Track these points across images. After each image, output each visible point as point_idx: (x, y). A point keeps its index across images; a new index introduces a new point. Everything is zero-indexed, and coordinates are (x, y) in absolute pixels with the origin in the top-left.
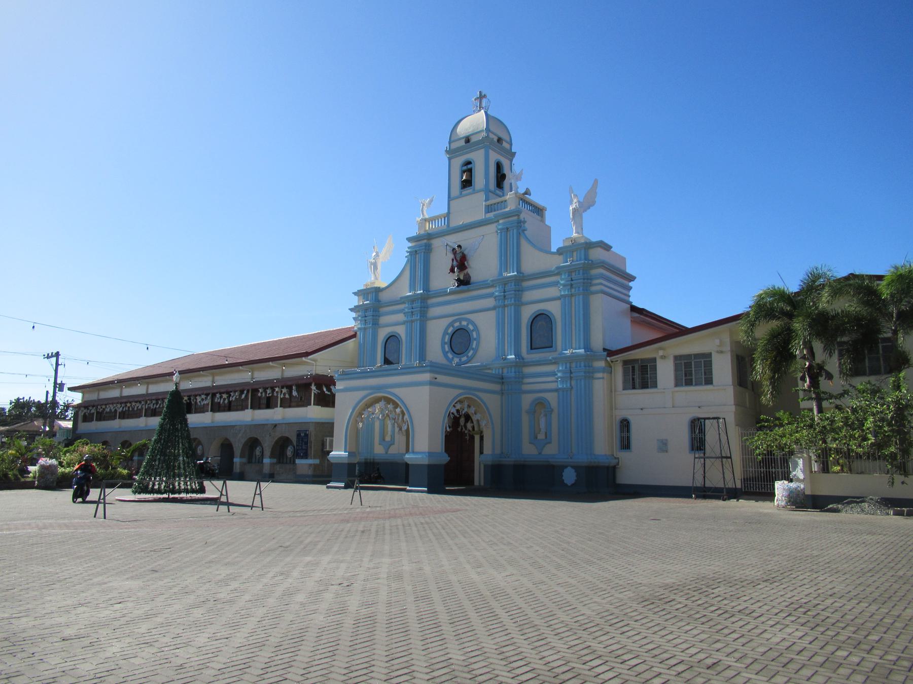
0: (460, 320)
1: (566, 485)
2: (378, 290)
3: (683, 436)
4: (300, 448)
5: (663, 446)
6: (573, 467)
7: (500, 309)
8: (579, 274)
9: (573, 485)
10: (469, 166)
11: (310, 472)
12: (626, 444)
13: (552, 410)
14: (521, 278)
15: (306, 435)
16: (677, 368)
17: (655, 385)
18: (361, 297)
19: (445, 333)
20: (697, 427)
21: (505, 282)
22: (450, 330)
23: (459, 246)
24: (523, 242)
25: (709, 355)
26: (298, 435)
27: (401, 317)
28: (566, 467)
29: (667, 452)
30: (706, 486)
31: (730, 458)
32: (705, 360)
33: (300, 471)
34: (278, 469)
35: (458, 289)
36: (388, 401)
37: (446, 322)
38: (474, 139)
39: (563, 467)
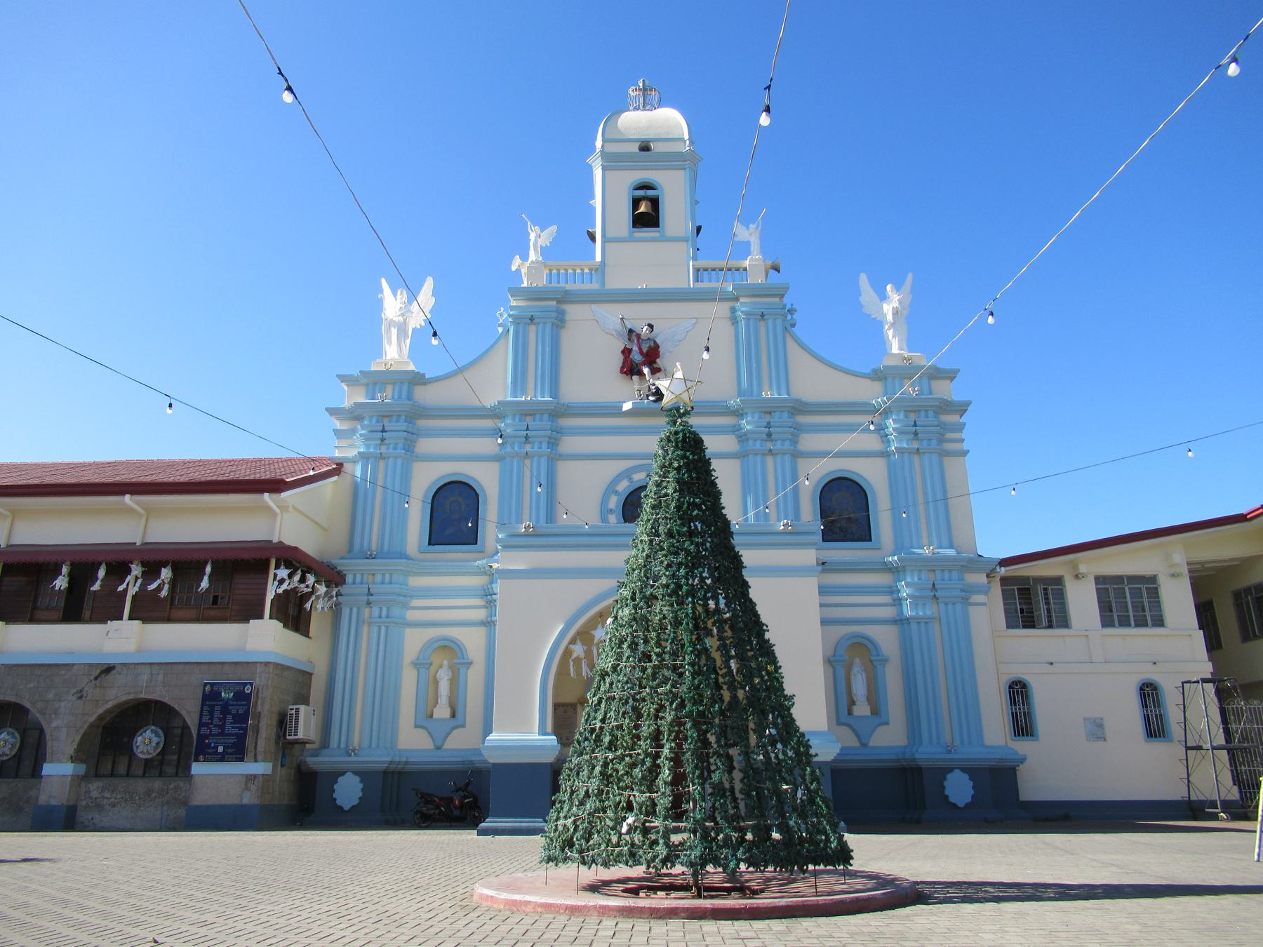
1: (954, 805)
3: (1131, 713)
4: (215, 731)
5: (1097, 730)
6: (964, 770)
7: (759, 458)
8: (927, 416)
9: (967, 805)
10: (650, 193)
11: (249, 798)
12: (1023, 726)
13: (885, 661)
14: (799, 408)
15: (242, 697)
17: (1065, 623)
18: (362, 390)
19: (610, 489)
20: (1149, 693)
21: (768, 409)
23: (651, 326)
24: (791, 344)
25: (1153, 579)
26: (210, 697)
28: (951, 770)
29: (1105, 740)
30: (1192, 798)
31: (1188, 748)
32: (1147, 587)
33: (202, 797)
34: (95, 794)
37: (614, 468)
38: (656, 147)
39: (941, 772)
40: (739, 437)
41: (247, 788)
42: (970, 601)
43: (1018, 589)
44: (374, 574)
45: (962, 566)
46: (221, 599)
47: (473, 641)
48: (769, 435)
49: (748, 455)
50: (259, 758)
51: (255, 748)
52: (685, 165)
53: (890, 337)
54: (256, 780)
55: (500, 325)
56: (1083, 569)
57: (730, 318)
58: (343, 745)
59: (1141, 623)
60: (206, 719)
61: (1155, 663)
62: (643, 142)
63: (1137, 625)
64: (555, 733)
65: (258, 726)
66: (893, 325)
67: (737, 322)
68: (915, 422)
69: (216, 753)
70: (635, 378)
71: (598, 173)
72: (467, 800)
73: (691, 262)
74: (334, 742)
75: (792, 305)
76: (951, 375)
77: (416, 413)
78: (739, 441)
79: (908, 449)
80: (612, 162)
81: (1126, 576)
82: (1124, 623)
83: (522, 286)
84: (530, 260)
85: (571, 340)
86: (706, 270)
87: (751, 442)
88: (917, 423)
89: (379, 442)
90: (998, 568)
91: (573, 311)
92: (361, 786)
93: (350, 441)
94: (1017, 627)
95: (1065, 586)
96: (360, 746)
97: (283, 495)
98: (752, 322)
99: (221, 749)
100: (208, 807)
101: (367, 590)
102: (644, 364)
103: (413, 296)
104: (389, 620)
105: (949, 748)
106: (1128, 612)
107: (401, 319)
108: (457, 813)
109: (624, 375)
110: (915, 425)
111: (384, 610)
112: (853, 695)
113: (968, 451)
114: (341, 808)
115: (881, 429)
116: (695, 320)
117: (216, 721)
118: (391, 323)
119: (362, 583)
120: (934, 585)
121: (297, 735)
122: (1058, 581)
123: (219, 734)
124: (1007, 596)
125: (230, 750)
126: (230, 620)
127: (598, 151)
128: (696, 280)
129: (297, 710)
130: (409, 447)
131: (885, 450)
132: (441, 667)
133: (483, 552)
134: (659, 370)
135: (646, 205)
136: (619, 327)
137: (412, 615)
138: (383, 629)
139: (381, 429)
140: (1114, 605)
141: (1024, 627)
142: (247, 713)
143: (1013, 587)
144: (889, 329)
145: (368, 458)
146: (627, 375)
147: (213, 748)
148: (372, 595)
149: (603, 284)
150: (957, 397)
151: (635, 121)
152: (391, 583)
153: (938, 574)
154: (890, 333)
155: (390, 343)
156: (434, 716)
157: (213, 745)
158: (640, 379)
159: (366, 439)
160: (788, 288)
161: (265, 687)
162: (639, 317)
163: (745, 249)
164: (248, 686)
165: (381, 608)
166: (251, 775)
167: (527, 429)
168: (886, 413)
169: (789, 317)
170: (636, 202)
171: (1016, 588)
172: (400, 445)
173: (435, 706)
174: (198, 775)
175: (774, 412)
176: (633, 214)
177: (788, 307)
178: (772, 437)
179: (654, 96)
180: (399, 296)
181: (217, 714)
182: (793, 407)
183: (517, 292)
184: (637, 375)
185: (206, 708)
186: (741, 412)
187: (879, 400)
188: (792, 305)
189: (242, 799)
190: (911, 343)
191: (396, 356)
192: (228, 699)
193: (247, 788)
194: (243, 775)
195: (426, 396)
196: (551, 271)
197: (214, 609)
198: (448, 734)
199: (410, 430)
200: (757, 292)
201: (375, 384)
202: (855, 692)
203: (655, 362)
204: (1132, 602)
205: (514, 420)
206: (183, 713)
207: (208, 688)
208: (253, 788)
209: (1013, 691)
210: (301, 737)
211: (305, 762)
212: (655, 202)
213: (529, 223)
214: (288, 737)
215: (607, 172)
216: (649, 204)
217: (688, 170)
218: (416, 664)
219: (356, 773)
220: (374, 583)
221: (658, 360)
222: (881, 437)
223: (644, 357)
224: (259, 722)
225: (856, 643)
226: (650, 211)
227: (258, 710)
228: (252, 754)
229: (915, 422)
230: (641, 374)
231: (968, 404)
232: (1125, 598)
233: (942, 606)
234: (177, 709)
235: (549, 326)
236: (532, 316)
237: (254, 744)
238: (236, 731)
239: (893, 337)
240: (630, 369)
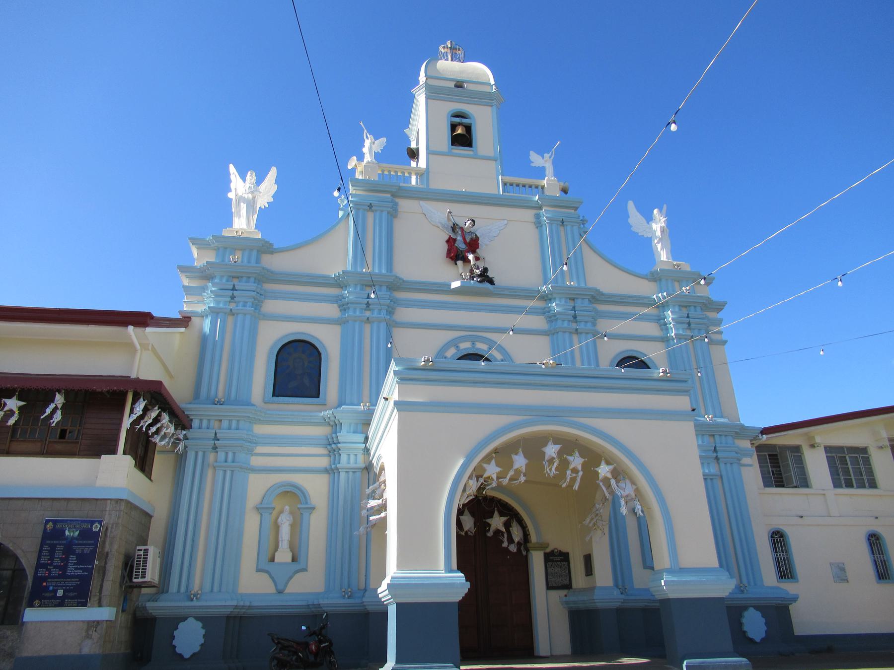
1: (751, 641)
4: (55, 572)
5: (841, 574)
7: (567, 335)
8: (696, 311)
9: (763, 640)
10: (464, 121)
12: (785, 571)
14: (597, 297)
15: (89, 535)
16: (831, 461)
21: (572, 296)
27: (331, 310)
28: (745, 608)
29: (848, 582)
35: (480, 285)
36: (569, 445)
41: (88, 636)
43: (769, 455)
44: (221, 421)
46: (70, 432)
48: (575, 317)
49: (558, 333)
50: (104, 602)
51: (100, 591)
53: (659, 249)
54: (99, 627)
55: (341, 209)
56: (818, 440)
58: (183, 589)
59: (861, 486)
60: (44, 560)
61: (877, 518)
62: (458, 82)
63: (858, 487)
64: (460, 568)
65: (105, 567)
66: (661, 240)
67: (542, 226)
69: (55, 597)
70: (460, 263)
72: (324, 645)
73: (500, 177)
74: (173, 587)
75: (583, 217)
77: (265, 277)
79: (684, 335)
80: (433, 93)
81: (846, 447)
82: (849, 485)
84: (365, 161)
85: (401, 227)
87: (559, 322)
88: (690, 315)
89: (229, 299)
90: (760, 435)
91: (404, 205)
92: (203, 632)
93: (199, 298)
94: (771, 486)
95: (803, 454)
96: (201, 589)
97: (149, 330)
98: (554, 226)
99: (60, 593)
100: (42, 659)
102: (468, 251)
103: (259, 181)
104: (234, 464)
105: (742, 588)
106: (850, 476)
107: (250, 196)
108: (312, 658)
110: (688, 317)
111: (230, 455)
114: (181, 656)
115: (660, 321)
117: (57, 562)
118: (240, 199)
119: (208, 428)
120: (715, 447)
121: (145, 577)
122: (797, 449)
123: (59, 577)
124: (761, 459)
125: (71, 594)
126: (78, 455)
128: (504, 191)
129: (146, 551)
130: (257, 305)
131: (665, 336)
132: (281, 512)
133: (325, 405)
135: (462, 129)
137: (256, 461)
138: (228, 473)
139: (231, 287)
140: (840, 470)
141: (777, 486)
142: (93, 552)
143: (765, 453)
144: (658, 243)
145: (218, 313)
147: (51, 592)
148: (218, 440)
149: (428, 185)
150: (715, 298)
151: (448, 66)
152: (237, 429)
154: (659, 246)
155: (239, 216)
156: (276, 560)
157: (51, 588)
158: (464, 265)
159: (216, 296)
161: (115, 525)
163: (540, 172)
164: (97, 524)
165: (227, 453)
166: (94, 622)
168: (663, 306)
170: (453, 127)
171: (767, 454)
172: (249, 304)
173: (276, 552)
174: (32, 622)
175: (577, 298)
176: (452, 134)
178: (577, 318)
179: (461, 53)
180: (248, 177)
181: (58, 554)
185: (46, 547)
186: (550, 297)
187: (660, 295)
189: (81, 650)
190: (674, 253)
191: (244, 226)
192: (73, 538)
193: (88, 636)
194: (83, 622)
197: (62, 442)
198: (291, 578)
200: (555, 203)
201: (226, 248)
204: (853, 468)
205: (355, 288)
206: (19, 553)
207: (50, 526)
208: (95, 635)
209: (774, 540)
210: (149, 580)
211: (145, 608)
212: (468, 128)
213: (365, 131)
214: (135, 580)
215: (429, 100)
216: (464, 129)
217: (495, 107)
218: (258, 509)
219: (198, 618)
220: (220, 428)
222: (660, 326)
224: (106, 563)
226: (465, 133)
227: (106, 550)
228: (97, 598)
229: (688, 314)
230: (466, 260)
231: (724, 304)
232: (847, 464)
233: (722, 465)
234: (11, 548)
235: (385, 214)
237: (99, 587)
238: (80, 572)
239: (661, 250)
240: (455, 255)
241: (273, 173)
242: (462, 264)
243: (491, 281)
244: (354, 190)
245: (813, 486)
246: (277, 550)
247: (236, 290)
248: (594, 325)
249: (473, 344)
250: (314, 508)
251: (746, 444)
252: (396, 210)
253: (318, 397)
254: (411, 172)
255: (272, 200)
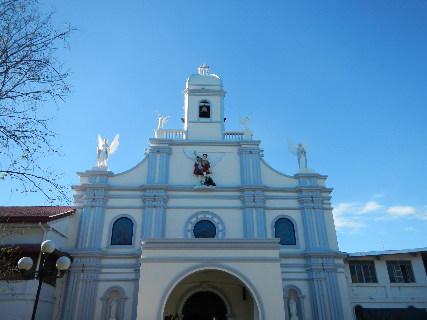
0: (205, 213)
2: (110, 174)
8: (317, 194)
10: (206, 104)
14: (266, 189)
17: (375, 280)
19: (189, 222)
22: (194, 220)
24: (262, 164)
27: (138, 202)
40: (242, 200)
42: (338, 271)
45: (334, 256)
47: (128, 288)
49: (246, 208)
52: (220, 95)
57: (238, 153)
68: (312, 196)
70: (199, 176)
71: (186, 96)
75: (262, 148)
76: (325, 177)
77: (109, 188)
78: (242, 202)
80: (191, 92)
83: (155, 138)
86: (228, 134)
91: (175, 148)
101: (82, 265)
109: (195, 174)
110: (312, 197)
112: (290, 313)
113: (333, 208)
116: (224, 154)
127: (186, 89)
134: (209, 173)
136: (194, 156)
139: (93, 195)
146: (196, 174)
148: (84, 267)
153: (324, 259)
158: (202, 176)
160: (261, 142)
162: (201, 151)
167: (155, 196)
169: (261, 153)
170: (201, 108)
175: (256, 190)
177: (261, 149)
178: (255, 200)
182: (263, 189)
183: (152, 140)
184: (200, 174)
188: (262, 148)
195: (112, 181)
196: (167, 133)
199: (105, 195)
202: (291, 311)
203: (208, 170)
212: (208, 108)
215: (190, 96)
221: (209, 169)
223: (203, 167)
225: (291, 289)
229: (312, 196)
230: (202, 174)
233: (326, 273)
236: (159, 150)
240: (197, 172)
241: (117, 137)
242: (201, 177)
243: (214, 185)
244: (152, 144)
245: (379, 283)
246: (110, 317)
247: (96, 196)
248: (265, 203)
249: (205, 215)
250: (127, 299)
251: (341, 262)
252: (171, 152)
253: (131, 244)
254: (180, 132)
255: (116, 149)
